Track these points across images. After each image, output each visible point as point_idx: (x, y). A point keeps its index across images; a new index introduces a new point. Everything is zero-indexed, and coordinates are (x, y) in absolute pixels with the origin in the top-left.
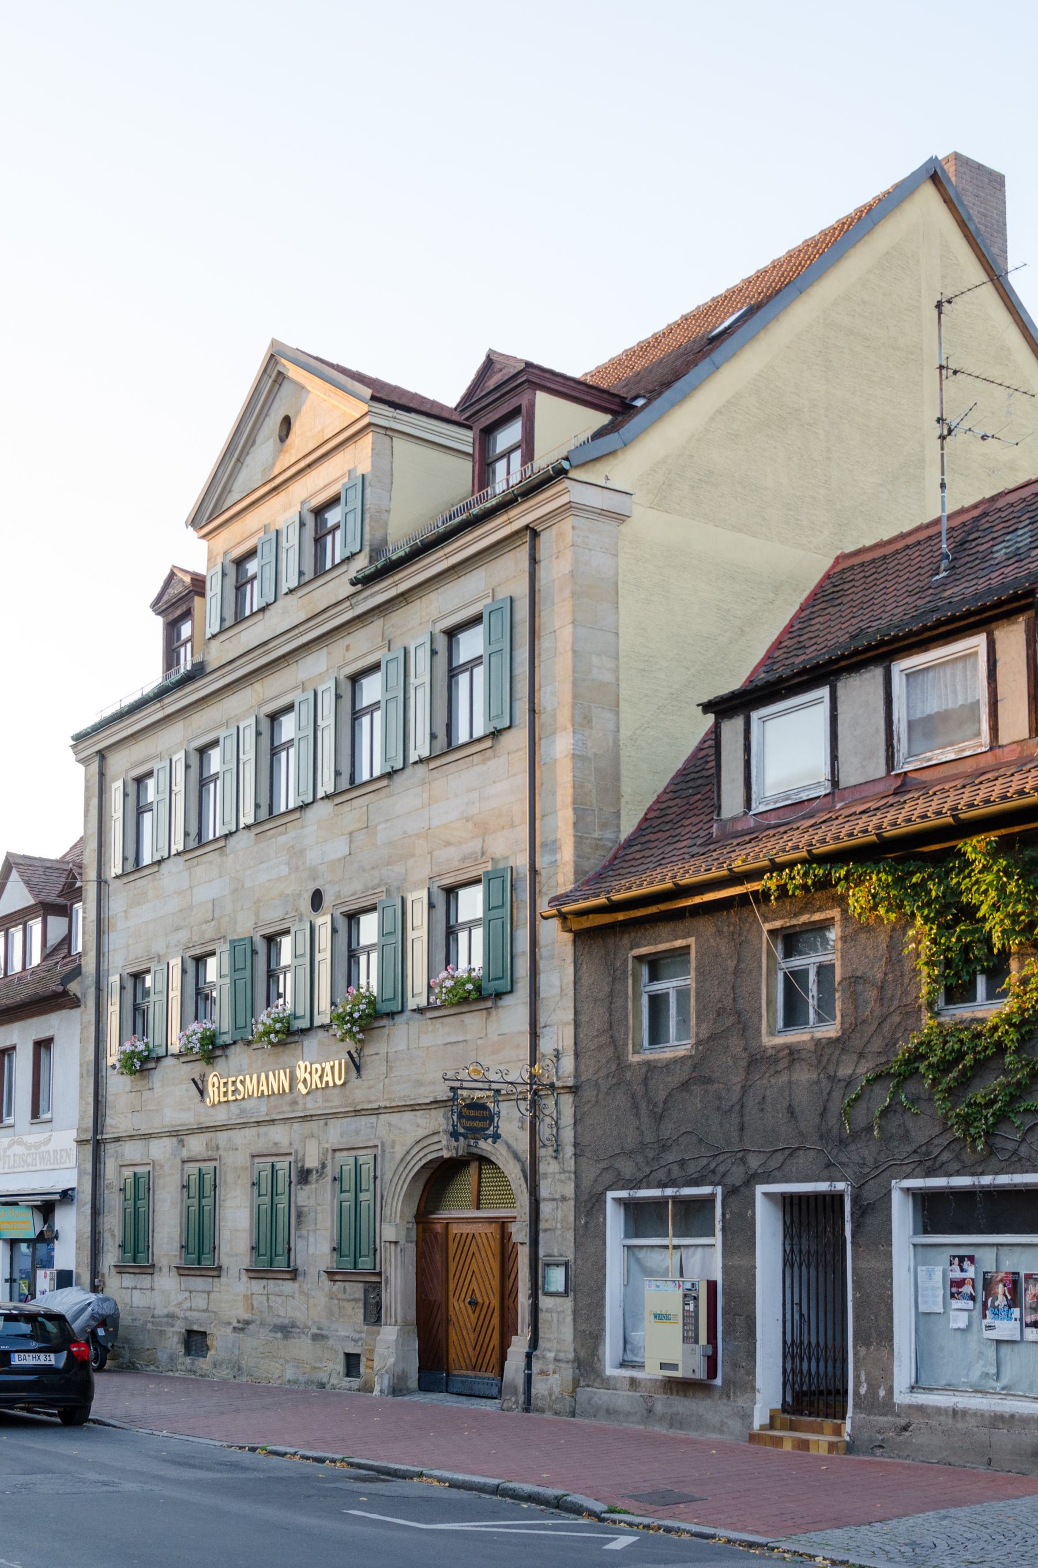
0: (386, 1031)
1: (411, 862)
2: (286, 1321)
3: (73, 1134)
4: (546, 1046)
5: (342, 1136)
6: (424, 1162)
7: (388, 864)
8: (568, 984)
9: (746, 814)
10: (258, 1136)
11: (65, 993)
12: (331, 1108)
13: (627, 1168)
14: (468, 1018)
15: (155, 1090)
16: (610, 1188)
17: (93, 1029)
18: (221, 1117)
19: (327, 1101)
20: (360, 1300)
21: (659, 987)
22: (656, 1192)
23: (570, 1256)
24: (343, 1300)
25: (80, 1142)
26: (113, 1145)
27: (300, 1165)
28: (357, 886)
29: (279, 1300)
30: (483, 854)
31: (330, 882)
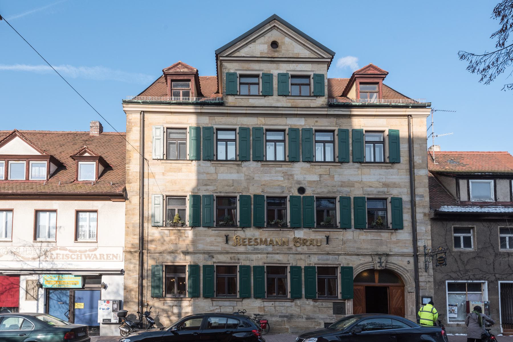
0: (342, 233)
2: (287, 314)
5: (318, 260)
10: (267, 257)
14: (382, 234)
16: (448, 280)
21: (503, 235)
22: (466, 281)
23: (432, 295)
28: (325, 190)
30: (387, 192)
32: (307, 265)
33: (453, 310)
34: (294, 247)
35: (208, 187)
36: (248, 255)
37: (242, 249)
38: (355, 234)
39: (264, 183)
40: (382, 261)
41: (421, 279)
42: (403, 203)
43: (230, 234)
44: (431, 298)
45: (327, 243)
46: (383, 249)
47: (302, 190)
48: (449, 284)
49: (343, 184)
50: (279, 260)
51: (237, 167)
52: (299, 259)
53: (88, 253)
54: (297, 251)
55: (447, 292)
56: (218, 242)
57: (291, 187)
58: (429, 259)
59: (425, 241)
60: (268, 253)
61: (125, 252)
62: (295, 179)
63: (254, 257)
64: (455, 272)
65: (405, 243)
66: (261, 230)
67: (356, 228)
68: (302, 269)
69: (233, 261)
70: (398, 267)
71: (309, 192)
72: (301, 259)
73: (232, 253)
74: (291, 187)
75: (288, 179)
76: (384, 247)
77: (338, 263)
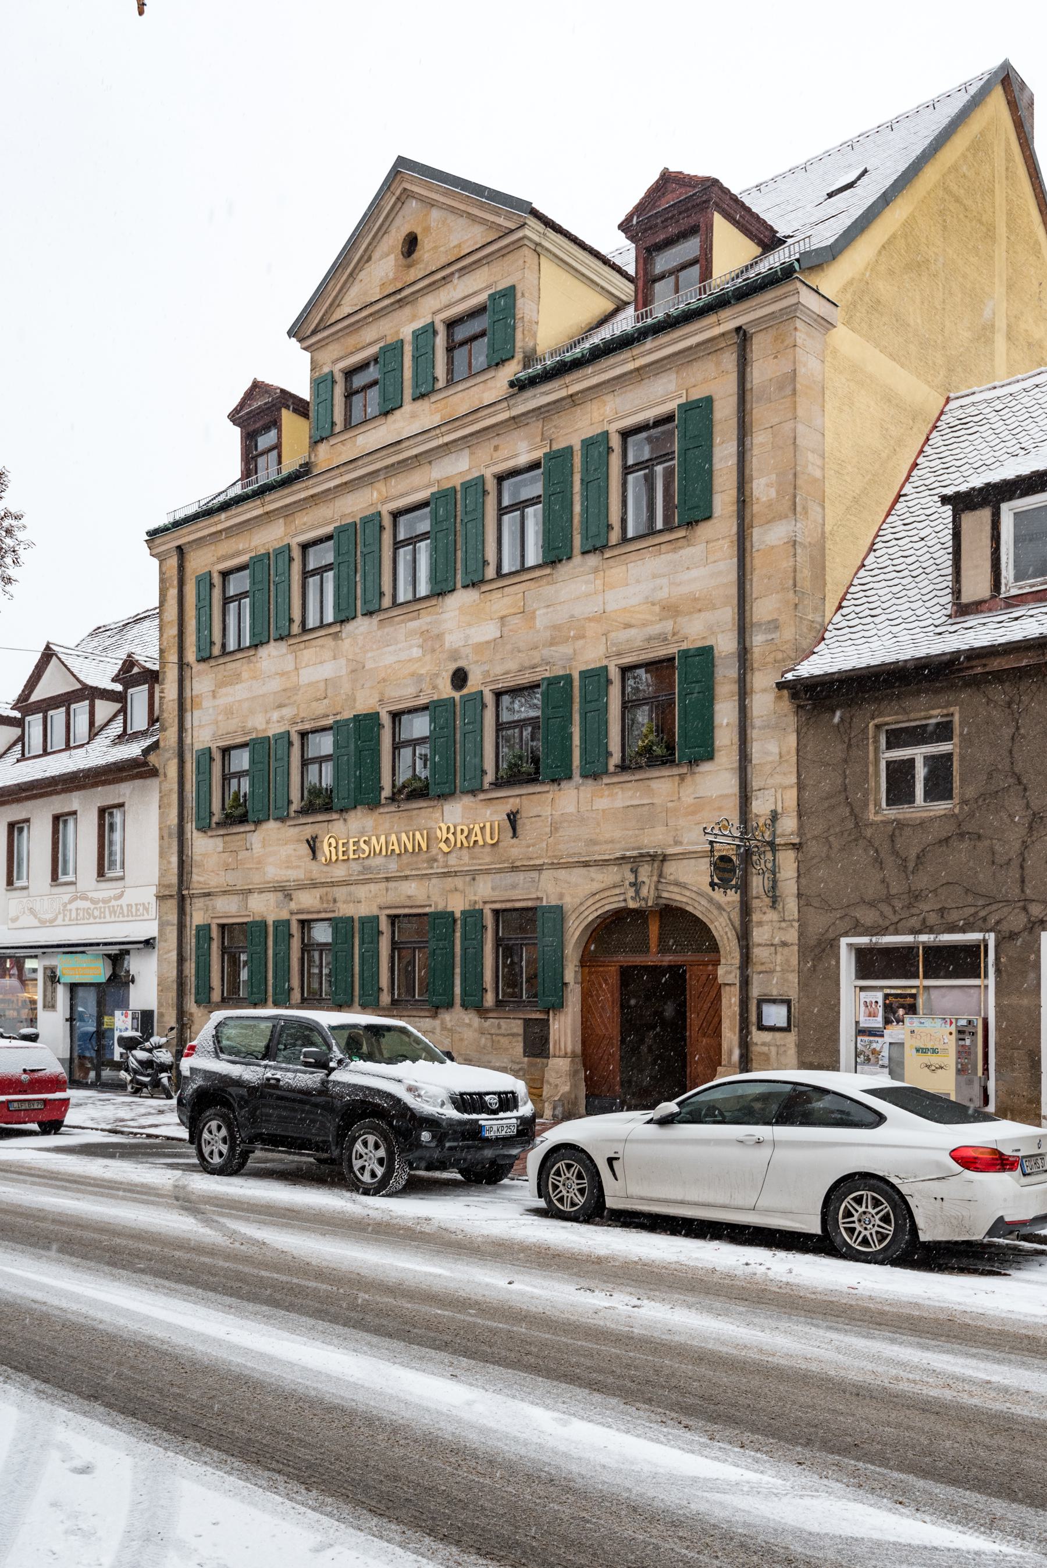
0: (550, 796)
1: (581, 642)
3: (153, 890)
4: (760, 807)
5: (493, 889)
6: (599, 912)
7: (551, 644)
8: (789, 753)
9: (993, 597)
10: (387, 890)
11: (146, 764)
12: (480, 865)
13: (868, 916)
14: (655, 785)
15: (254, 851)
16: (846, 934)
17: (175, 797)
18: (339, 872)
19: (473, 858)
22: (909, 939)
25: (161, 898)
26: (202, 900)
28: (512, 665)
31: (477, 662)
32: (467, 908)
33: (874, 1052)
36: (353, 887)
38: (581, 795)
39: (383, 675)
40: (640, 879)
41: (759, 935)
42: (717, 662)
43: (320, 833)
45: (515, 835)
46: (654, 839)
47: (460, 678)
49: (557, 635)
50: (409, 897)
52: (451, 891)
53: (113, 903)
54: (446, 866)
56: (300, 857)
57: (437, 675)
59: (777, 795)
60: (388, 879)
61: (157, 897)
62: (447, 645)
63: (361, 891)
64: (872, 904)
65: (720, 809)
67: (584, 776)
68: (455, 921)
69: (325, 905)
70: (694, 896)
71: (474, 684)
72: (456, 890)
73: (323, 884)
74: (437, 675)
75: (433, 650)
76: (660, 829)
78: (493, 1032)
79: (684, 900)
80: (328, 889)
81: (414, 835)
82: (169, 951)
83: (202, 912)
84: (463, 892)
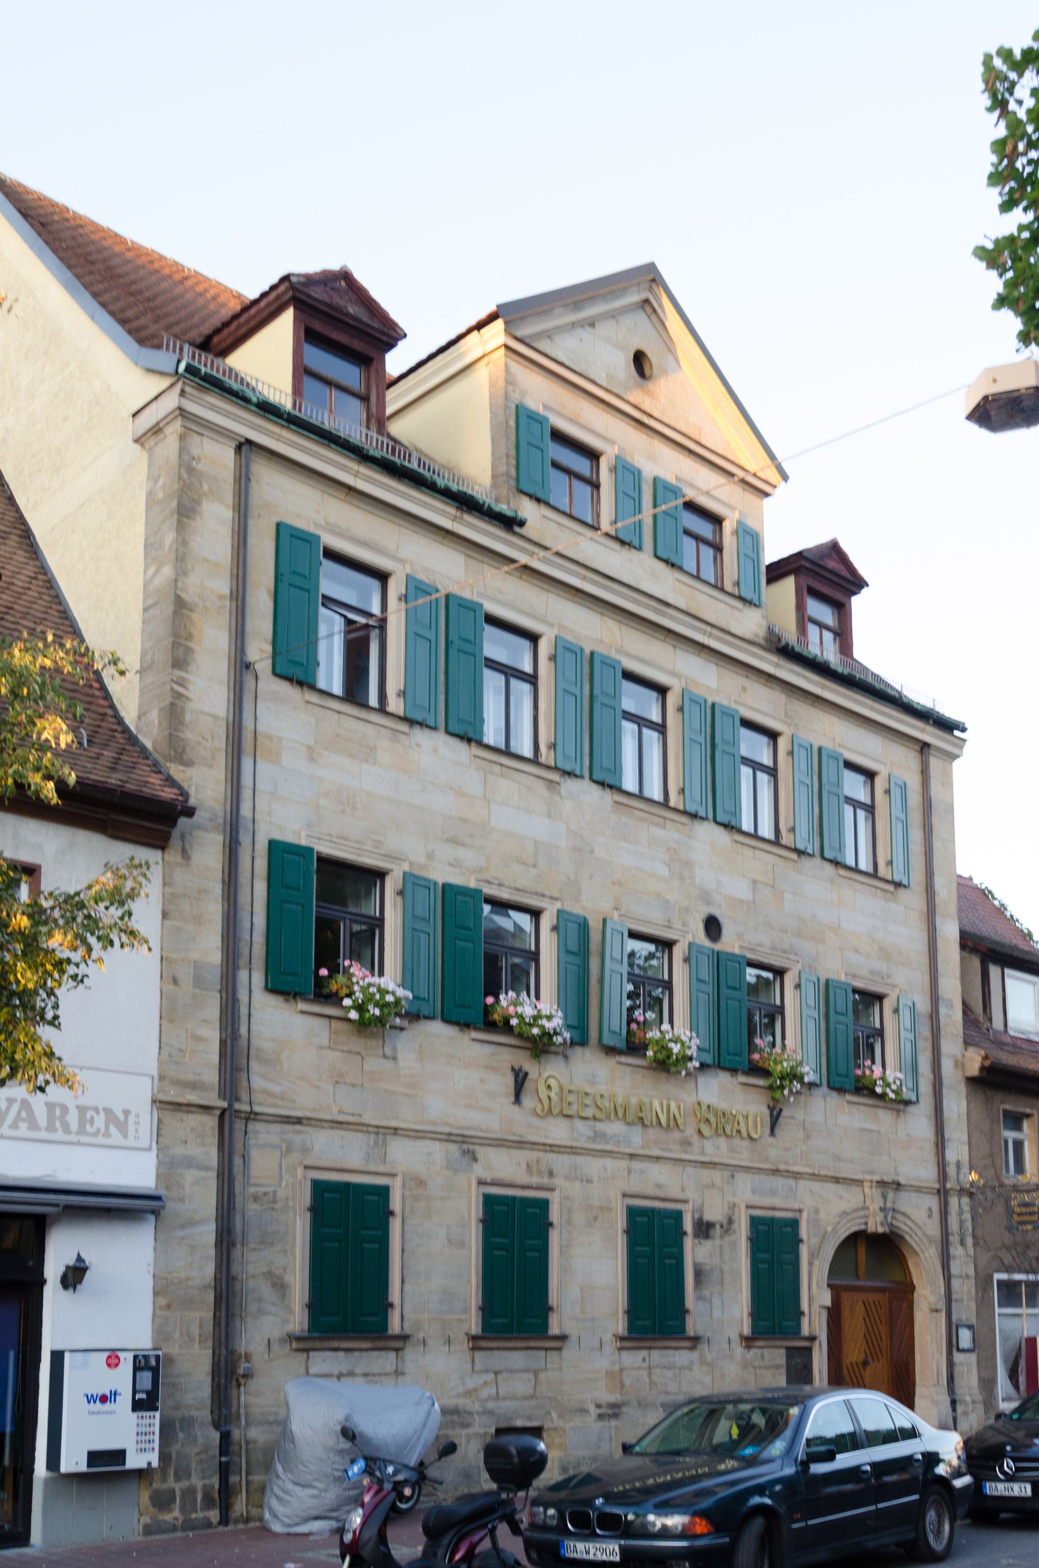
5: (753, 1191)
10: (629, 1171)
16: (997, 1271)
17: (214, 910)
18: (558, 1132)
20: (781, 1366)
23: (974, 1321)
24: (760, 1368)
25: (167, 1106)
26: (277, 1128)
27: (697, 1216)
29: (669, 1374)
34: (695, 1139)
35: (462, 853)
36: (579, 1159)
37: (558, 1132)
44: (970, 1327)
45: (772, 1133)
47: (713, 926)
48: (999, 1282)
50: (659, 1186)
51: (546, 793)
55: (997, 1310)
57: (687, 910)
58: (965, 1200)
61: (154, 1102)
63: (593, 1166)
66: (612, 1061)
69: (535, 1180)
71: (730, 942)
73: (534, 1145)
75: (681, 878)
77: (796, 1206)
78: (756, 1364)
79: (906, 1229)
80: (541, 1154)
81: (669, 1107)
82: (192, 1223)
83: (278, 1154)
84: (721, 1190)
